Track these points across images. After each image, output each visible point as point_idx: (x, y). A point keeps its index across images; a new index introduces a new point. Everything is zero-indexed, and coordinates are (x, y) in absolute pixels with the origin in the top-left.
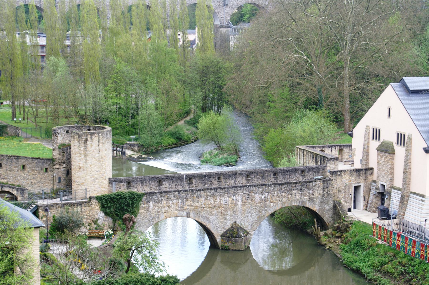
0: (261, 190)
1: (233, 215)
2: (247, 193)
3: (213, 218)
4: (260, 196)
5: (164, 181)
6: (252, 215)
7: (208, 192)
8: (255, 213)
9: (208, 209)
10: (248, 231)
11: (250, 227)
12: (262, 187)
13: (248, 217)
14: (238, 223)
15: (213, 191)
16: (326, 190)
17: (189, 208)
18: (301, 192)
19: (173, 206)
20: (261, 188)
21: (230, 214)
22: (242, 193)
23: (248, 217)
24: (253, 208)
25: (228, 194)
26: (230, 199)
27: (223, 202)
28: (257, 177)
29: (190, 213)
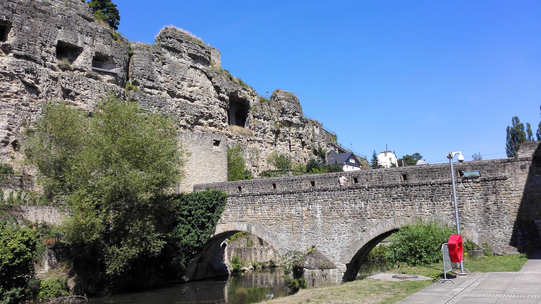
0: (352, 196)
1: (310, 234)
2: (330, 200)
3: (282, 236)
4: (353, 206)
5: (244, 187)
6: (341, 237)
7: (273, 198)
8: (345, 233)
9: (274, 223)
10: (336, 263)
11: (338, 258)
12: (354, 191)
13: (333, 240)
14: (319, 249)
15: (279, 196)
16: (493, 198)
17: (250, 219)
18: (432, 201)
19: (230, 216)
20: (352, 192)
21: (305, 232)
22: (322, 200)
23: (333, 240)
24: (342, 225)
25: (300, 201)
26: (305, 209)
27: (293, 212)
28: (370, 181)
29: (251, 226)
